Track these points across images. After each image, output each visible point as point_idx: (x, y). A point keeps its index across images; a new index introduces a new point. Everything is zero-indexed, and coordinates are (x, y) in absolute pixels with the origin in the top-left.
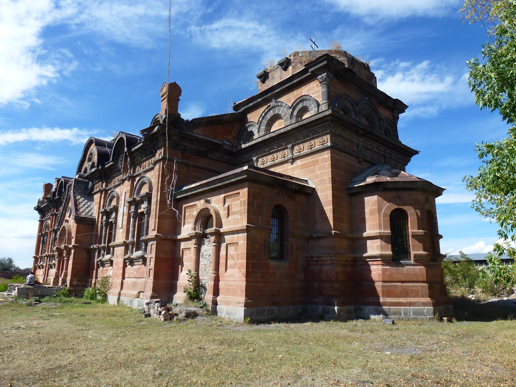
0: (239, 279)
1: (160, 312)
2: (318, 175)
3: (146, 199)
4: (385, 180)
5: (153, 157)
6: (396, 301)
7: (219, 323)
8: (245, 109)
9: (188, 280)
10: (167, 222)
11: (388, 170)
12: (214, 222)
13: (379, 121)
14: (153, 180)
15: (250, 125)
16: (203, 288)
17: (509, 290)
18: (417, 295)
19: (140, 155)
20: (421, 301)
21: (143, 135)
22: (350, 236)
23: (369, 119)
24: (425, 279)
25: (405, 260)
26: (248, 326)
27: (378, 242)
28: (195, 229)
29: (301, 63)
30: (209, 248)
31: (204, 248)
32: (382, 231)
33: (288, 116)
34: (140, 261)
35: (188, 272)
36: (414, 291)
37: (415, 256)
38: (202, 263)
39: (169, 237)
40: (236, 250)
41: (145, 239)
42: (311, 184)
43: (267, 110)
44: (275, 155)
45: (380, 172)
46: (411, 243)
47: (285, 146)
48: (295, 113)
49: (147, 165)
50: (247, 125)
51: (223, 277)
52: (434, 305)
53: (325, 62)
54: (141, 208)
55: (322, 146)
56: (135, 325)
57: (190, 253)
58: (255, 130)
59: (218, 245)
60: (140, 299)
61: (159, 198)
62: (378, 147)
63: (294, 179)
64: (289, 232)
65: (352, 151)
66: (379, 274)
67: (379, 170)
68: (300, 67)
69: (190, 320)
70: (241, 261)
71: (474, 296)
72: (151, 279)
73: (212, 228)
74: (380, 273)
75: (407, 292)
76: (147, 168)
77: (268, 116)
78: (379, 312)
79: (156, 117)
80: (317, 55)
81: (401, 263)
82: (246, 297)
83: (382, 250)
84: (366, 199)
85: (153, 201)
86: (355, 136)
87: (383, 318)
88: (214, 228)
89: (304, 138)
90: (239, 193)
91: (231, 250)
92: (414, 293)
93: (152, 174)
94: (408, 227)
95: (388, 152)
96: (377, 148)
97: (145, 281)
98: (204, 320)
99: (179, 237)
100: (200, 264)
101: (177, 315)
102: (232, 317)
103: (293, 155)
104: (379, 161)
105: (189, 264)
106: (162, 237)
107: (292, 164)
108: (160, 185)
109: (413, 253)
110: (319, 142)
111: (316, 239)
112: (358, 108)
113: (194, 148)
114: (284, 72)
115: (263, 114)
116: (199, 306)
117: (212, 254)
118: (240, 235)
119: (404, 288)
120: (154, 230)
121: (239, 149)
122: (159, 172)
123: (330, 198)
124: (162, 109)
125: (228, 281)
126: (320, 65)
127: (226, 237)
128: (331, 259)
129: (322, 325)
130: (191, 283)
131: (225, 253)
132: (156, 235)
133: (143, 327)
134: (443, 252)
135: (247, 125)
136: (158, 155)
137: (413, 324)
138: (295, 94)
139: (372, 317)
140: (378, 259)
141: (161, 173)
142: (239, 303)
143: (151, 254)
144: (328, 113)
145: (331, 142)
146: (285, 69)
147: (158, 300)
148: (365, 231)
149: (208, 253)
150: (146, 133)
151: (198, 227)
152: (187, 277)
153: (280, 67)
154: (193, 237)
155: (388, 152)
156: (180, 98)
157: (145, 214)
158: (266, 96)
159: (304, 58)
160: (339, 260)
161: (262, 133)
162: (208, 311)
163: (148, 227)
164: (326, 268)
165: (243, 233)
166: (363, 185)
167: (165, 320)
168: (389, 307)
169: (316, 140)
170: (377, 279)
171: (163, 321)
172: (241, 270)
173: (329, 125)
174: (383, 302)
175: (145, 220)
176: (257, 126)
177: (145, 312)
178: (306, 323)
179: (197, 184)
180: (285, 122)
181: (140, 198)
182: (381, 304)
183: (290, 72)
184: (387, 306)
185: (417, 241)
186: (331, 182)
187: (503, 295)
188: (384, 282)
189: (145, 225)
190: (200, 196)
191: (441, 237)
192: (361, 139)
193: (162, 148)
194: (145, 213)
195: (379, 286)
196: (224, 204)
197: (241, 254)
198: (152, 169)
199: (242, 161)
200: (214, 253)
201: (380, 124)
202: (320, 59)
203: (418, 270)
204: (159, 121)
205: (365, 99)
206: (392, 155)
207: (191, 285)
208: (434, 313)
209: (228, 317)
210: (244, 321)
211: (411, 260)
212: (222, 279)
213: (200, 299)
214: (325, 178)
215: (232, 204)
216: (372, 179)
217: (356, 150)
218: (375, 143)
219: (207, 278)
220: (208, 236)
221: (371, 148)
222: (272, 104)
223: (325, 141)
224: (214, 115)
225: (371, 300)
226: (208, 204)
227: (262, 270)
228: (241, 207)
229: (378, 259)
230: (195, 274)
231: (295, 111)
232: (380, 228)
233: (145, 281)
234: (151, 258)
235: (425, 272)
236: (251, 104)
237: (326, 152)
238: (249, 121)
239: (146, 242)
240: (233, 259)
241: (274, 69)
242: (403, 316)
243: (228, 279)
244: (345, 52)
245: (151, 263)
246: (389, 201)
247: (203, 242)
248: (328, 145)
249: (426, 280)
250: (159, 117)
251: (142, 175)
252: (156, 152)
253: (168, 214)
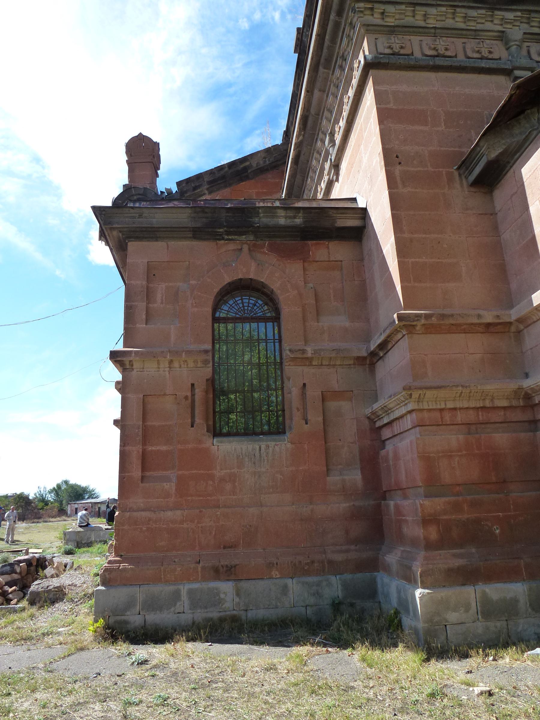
160: (441, 410)
192: (510, 15)
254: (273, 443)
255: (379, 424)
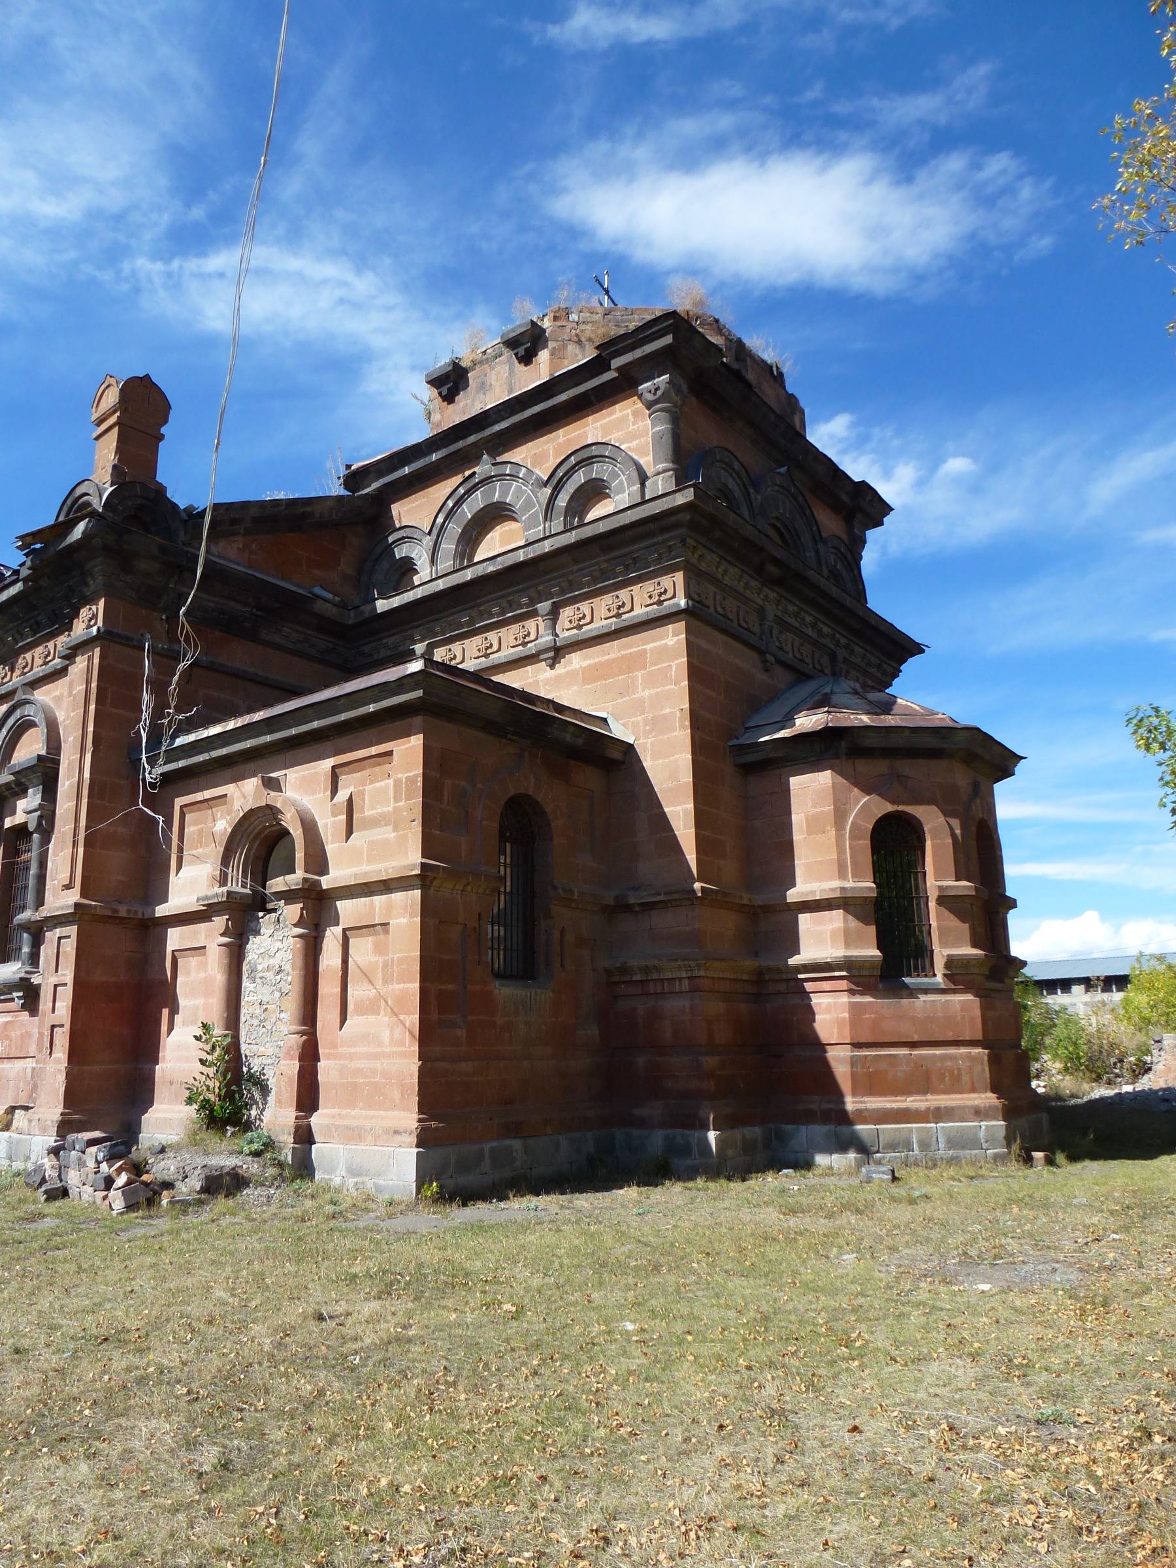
0: (395, 1049)
1: (109, 1182)
2: (641, 701)
3: (35, 781)
4: (856, 723)
5: (61, 633)
6: (895, 1105)
7: (330, 1209)
8: (385, 485)
9: (201, 1060)
10: (117, 860)
11: (856, 693)
12: (300, 855)
13: (816, 544)
14: (63, 713)
15: (403, 538)
16: (255, 1084)
17: (1135, 1065)
18: (955, 1087)
19: (11, 625)
20: (970, 1103)
21: (27, 555)
22: (745, 902)
23: (788, 537)
24: (979, 1036)
25: (918, 976)
26: (434, 1213)
27: (836, 919)
28: (223, 880)
29: (579, 342)
30: (278, 944)
31: (255, 947)
32: (850, 884)
33: (538, 509)
34: (12, 1000)
35: (199, 1032)
36: (947, 1074)
37: (950, 963)
38: (250, 998)
39: (123, 911)
40: (379, 949)
41: (33, 919)
42: (619, 731)
43: (462, 491)
44: (493, 636)
45: (835, 699)
46: (934, 923)
47: (527, 605)
48: (562, 501)
49: (38, 661)
50: (391, 540)
51: (334, 1046)
52: (1009, 1114)
53: (668, 339)
54: (13, 813)
55: (655, 607)
56: (17, 1235)
57: (203, 966)
58: (420, 554)
59: (314, 934)
60: (15, 1135)
61: (87, 775)
62: (815, 624)
63: (567, 712)
64: (555, 888)
65: (746, 629)
66: (840, 1023)
67: (827, 694)
68: (576, 355)
69: (222, 1203)
70: (402, 985)
71: (1042, 1084)
72: (58, 1061)
73: (292, 876)
74: (844, 1019)
75: (927, 1075)
76: (38, 671)
77: (468, 511)
78: (842, 1145)
79: (79, 491)
80: (630, 321)
81: (906, 986)
82: (420, 1112)
83: (847, 945)
84: (795, 782)
85: (66, 784)
86: (754, 584)
87: (859, 1165)
88: (300, 874)
89: (595, 581)
90: (390, 753)
91: (361, 949)
92: (947, 1079)
93: (57, 693)
94: (925, 873)
95: (843, 641)
96: (814, 625)
97: (33, 1069)
98: (269, 1198)
99: (161, 911)
100: (243, 1003)
101: (168, 1185)
102: (370, 1184)
103: (557, 635)
104: (818, 666)
105: (200, 1001)
106: (99, 912)
107: (552, 667)
108: (91, 729)
109: (940, 954)
110: (646, 596)
111: (637, 909)
112: (759, 497)
113: (212, 605)
114: (520, 368)
115: (450, 503)
116: (246, 1150)
117: (287, 967)
118: (398, 897)
119: (918, 1063)
120: (68, 887)
121: (367, 615)
122: (88, 682)
123: (687, 777)
124: (100, 466)
125: (351, 1057)
126: (649, 348)
127: (344, 907)
128: (689, 975)
129: (672, 1193)
130: (211, 1071)
131: (337, 961)
132: (77, 905)
133: (53, 1243)
134: (1017, 949)
135: (391, 540)
136: (84, 626)
137: (953, 1179)
138: (561, 440)
139: (821, 1160)
140: (837, 974)
141: (94, 685)
142: (396, 1132)
143: (57, 971)
144: (681, 499)
145: (688, 596)
146: (527, 358)
147: (97, 1134)
148: (793, 885)
149: (271, 961)
150: (38, 546)
151: (235, 873)
152: (196, 1051)
153: (508, 354)
154: (217, 908)
155: (843, 641)
156: (163, 430)
157: (32, 833)
158: (461, 444)
159: (588, 327)
160: (713, 978)
161: (446, 564)
162: (281, 1165)
163: (42, 879)
164: (676, 1005)
165: (406, 889)
166: (786, 735)
167: (130, 1207)
168: (873, 1127)
169: (636, 588)
170: (835, 1036)
171: (122, 1214)
172: (402, 1017)
173: (683, 541)
174: (857, 1110)
175: (34, 854)
176: (428, 541)
177: (43, 1181)
178: (621, 1192)
179: (231, 725)
180: (527, 528)
181: (12, 778)
182: (851, 1116)
183: (543, 369)
184: (868, 1123)
185: (952, 917)
186: (687, 723)
187: (1119, 1080)
188: (857, 1045)
189: (33, 870)
190: (240, 768)
191: (1012, 904)
192: (772, 595)
193: (99, 599)
194: (31, 827)
195: (840, 1059)
196: (334, 791)
197: (401, 961)
198: (61, 673)
199: (376, 657)
200: (299, 962)
201: (817, 552)
202: (651, 328)
203: (958, 1007)
204: (88, 504)
205: (778, 470)
206: (852, 652)
207: (211, 1075)
208: (1009, 1140)
209: (356, 1183)
210: (417, 1194)
211: (935, 975)
212: (327, 1051)
213: (247, 1126)
214: (668, 710)
215: (362, 793)
216: (814, 718)
217: (756, 629)
218: (808, 610)
219: (270, 1052)
220: (270, 906)
221: (797, 625)
222: (483, 468)
223: (666, 591)
224: (281, 496)
225: (814, 1107)
226: (273, 794)
227: (470, 1018)
228: (396, 800)
229: (837, 974)
230: (226, 1036)
231: (560, 496)
232: (842, 875)
233: (33, 1069)
234: (56, 986)
235: (977, 1012)
236: (407, 470)
237: (670, 626)
238: (398, 526)
239: (37, 932)
240: (370, 981)
241: (486, 359)
242: (916, 1152)
243: (352, 1050)
244: (717, 321)
245: (57, 1004)
246: (868, 792)
247: (252, 925)
248: (678, 605)
249: (981, 1038)
250: (91, 492)
251: (19, 696)
252: (77, 615)
253: (120, 830)
254: (539, 991)
255: (617, 979)
